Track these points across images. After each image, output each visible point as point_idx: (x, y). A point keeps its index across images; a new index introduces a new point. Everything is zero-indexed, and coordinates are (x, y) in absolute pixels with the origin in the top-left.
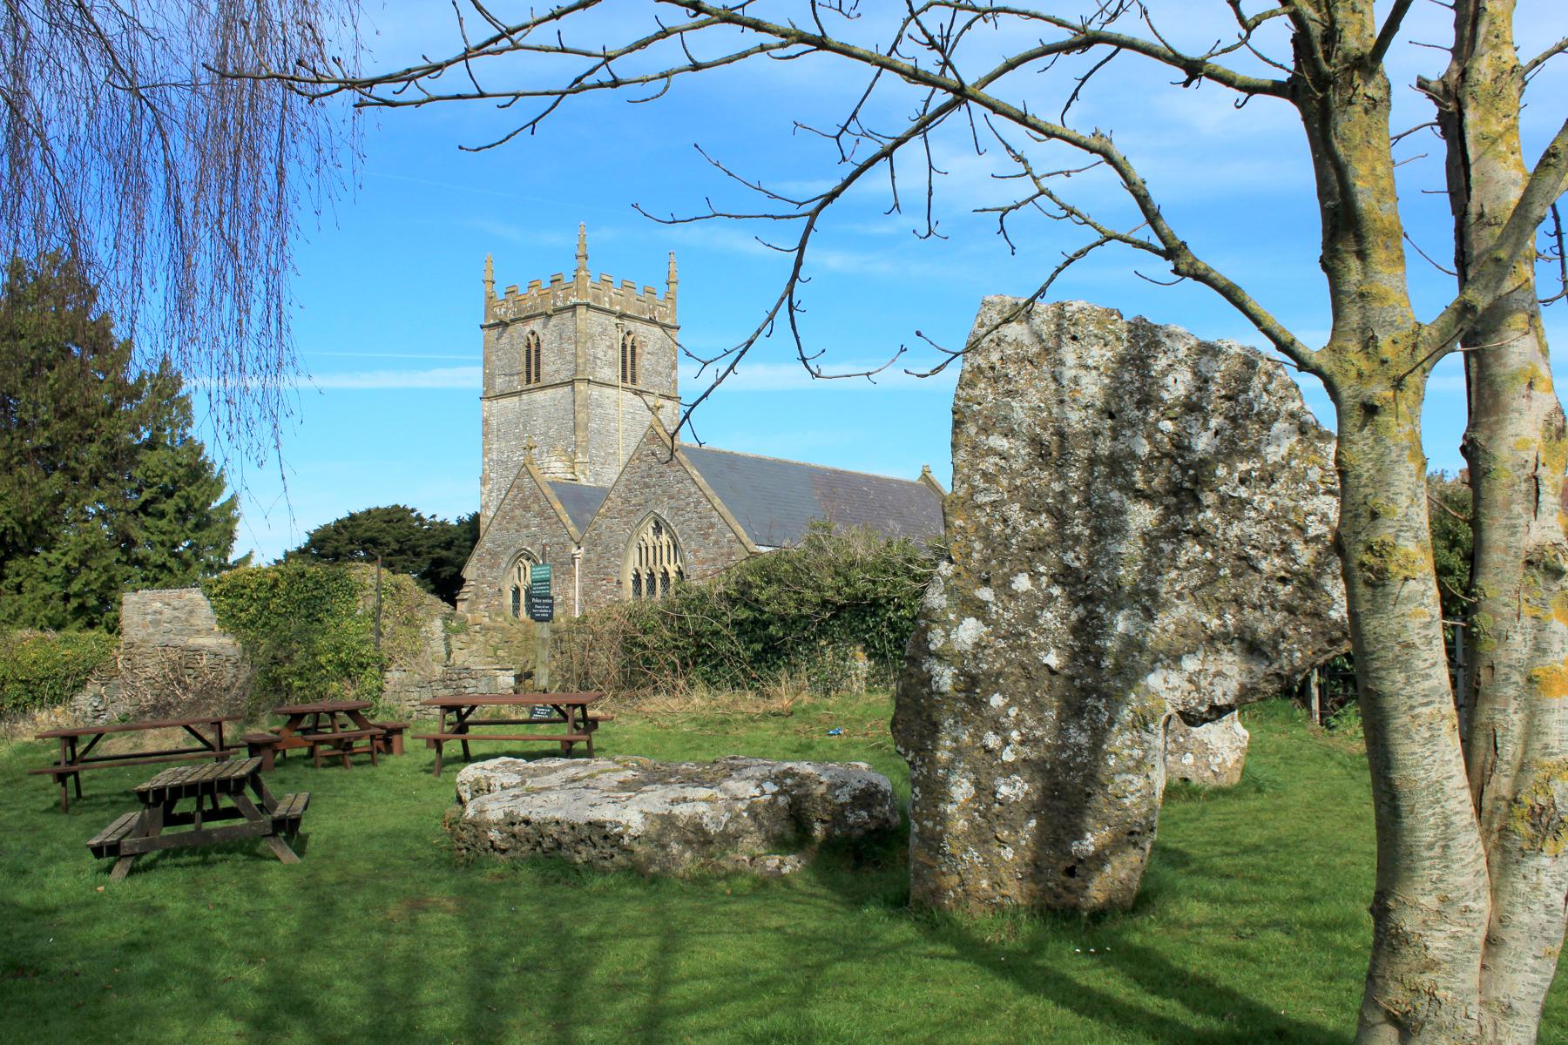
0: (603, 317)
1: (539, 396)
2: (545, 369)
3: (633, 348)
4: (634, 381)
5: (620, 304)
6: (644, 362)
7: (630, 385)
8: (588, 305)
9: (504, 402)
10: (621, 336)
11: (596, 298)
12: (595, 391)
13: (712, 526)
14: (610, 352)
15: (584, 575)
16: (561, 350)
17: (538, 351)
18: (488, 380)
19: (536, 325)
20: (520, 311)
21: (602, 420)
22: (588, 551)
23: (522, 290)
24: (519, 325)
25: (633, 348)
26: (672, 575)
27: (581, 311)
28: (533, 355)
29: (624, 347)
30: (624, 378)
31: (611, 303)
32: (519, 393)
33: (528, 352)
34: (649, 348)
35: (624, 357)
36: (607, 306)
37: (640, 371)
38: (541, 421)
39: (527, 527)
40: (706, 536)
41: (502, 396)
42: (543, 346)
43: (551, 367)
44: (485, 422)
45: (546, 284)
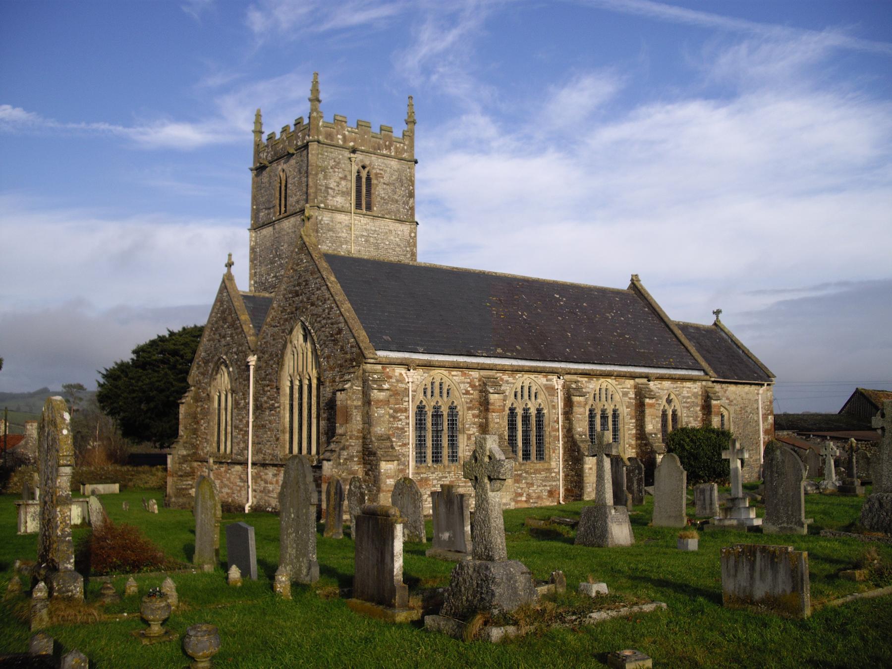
3: (369, 179)
4: (369, 207)
5: (354, 140)
6: (380, 191)
7: (364, 211)
8: (319, 142)
10: (355, 168)
11: (329, 136)
12: (326, 218)
14: (343, 183)
15: (256, 382)
16: (300, 183)
17: (286, 186)
18: (255, 215)
20: (275, 154)
21: (333, 242)
22: (259, 359)
23: (278, 136)
24: (274, 165)
25: (369, 179)
27: (313, 147)
29: (359, 178)
30: (358, 205)
31: (345, 138)
33: (280, 188)
34: (386, 179)
36: (341, 142)
37: (376, 199)
38: (286, 246)
39: (224, 337)
42: (290, 181)
45: (292, 129)
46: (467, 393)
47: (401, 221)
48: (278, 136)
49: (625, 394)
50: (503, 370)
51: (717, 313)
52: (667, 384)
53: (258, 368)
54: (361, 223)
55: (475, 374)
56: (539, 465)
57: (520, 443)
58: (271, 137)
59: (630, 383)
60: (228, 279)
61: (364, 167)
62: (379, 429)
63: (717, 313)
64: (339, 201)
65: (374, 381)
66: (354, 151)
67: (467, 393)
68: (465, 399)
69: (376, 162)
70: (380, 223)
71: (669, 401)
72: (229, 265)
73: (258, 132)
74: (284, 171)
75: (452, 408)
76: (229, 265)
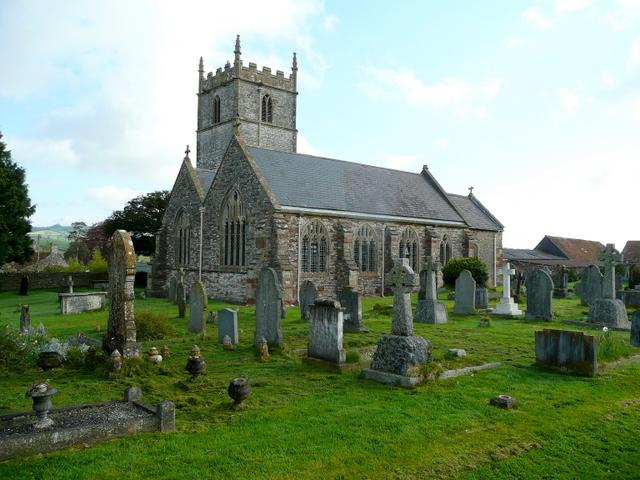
0: (249, 86)
1: (220, 129)
2: (222, 115)
3: (270, 103)
4: (270, 120)
6: (276, 110)
9: (206, 133)
10: (261, 97)
11: (246, 76)
12: (244, 126)
13: (258, 194)
14: (254, 105)
16: (228, 105)
19: (218, 92)
23: (214, 74)
26: (241, 223)
28: (217, 105)
29: (264, 102)
30: (264, 119)
31: (256, 79)
32: (211, 128)
34: (279, 104)
35: (264, 109)
40: (255, 200)
41: (205, 129)
43: (225, 113)
44: (198, 143)
45: (223, 70)
46: (331, 231)
47: (288, 130)
48: (214, 74)
49: (420, 234)
50: (352, 219)
51: (471, 189)
52: (444, 229)
53: (206, 215)
54: (265, 130)
55: (335, 221)
56: (371, 274)
57: (361, 261)
58: (210, 75)
59: (423, 228)
60: (187, 159)
61: (267, 96)
62: (281, 252)
63: (471, 189)
64: (251, 116)
65: (279, 223)
66: (260, 85)
67: (331, 231)
68: (330, 235)
69: (274, 94)
70: (274, 131)
71: (445, 239)
72: (187, 152)
73: (201, 71)
74: (218, 96)
75: (323, 240)
76: (187, 152)
